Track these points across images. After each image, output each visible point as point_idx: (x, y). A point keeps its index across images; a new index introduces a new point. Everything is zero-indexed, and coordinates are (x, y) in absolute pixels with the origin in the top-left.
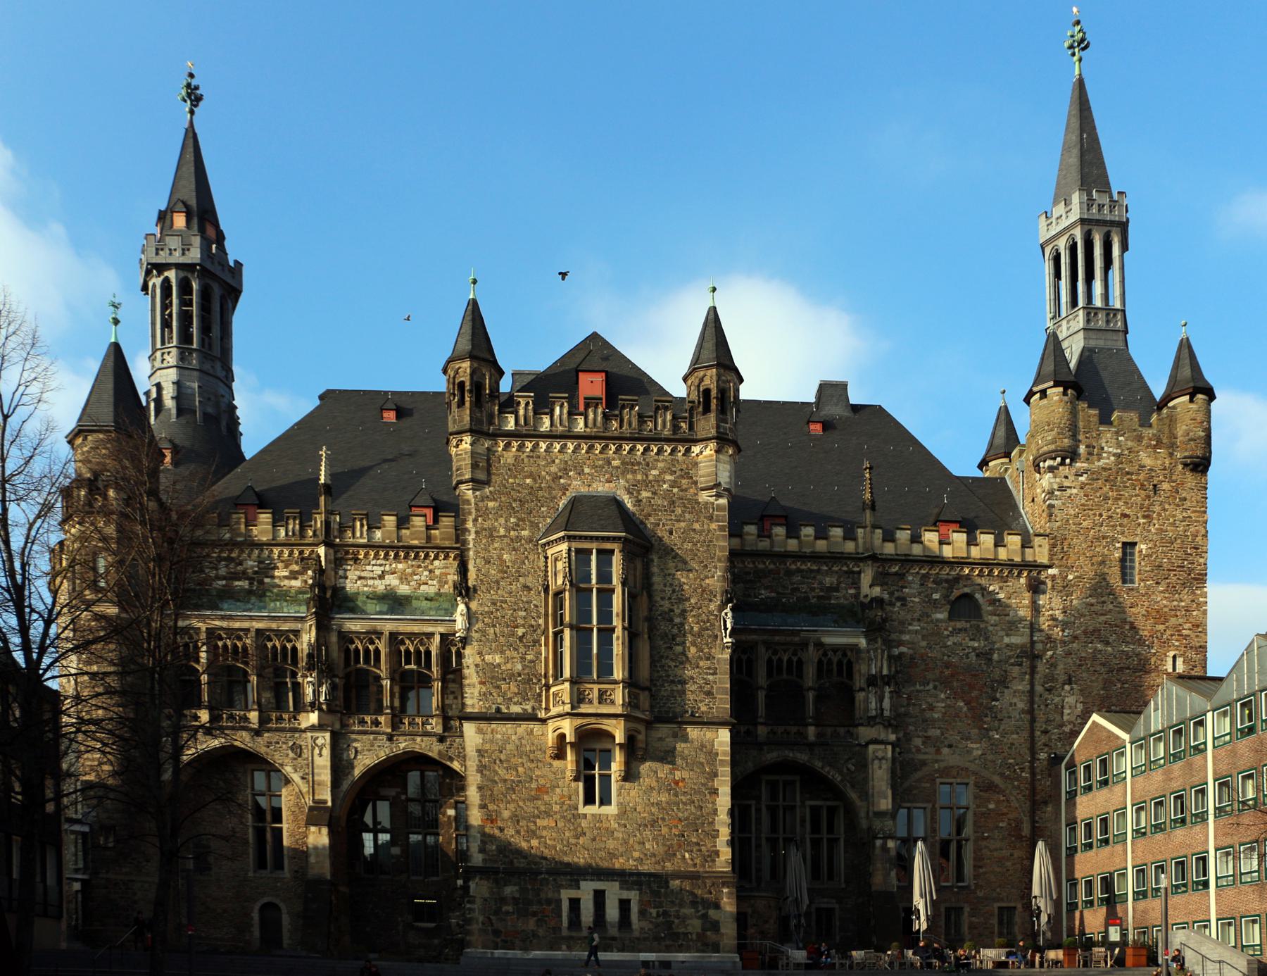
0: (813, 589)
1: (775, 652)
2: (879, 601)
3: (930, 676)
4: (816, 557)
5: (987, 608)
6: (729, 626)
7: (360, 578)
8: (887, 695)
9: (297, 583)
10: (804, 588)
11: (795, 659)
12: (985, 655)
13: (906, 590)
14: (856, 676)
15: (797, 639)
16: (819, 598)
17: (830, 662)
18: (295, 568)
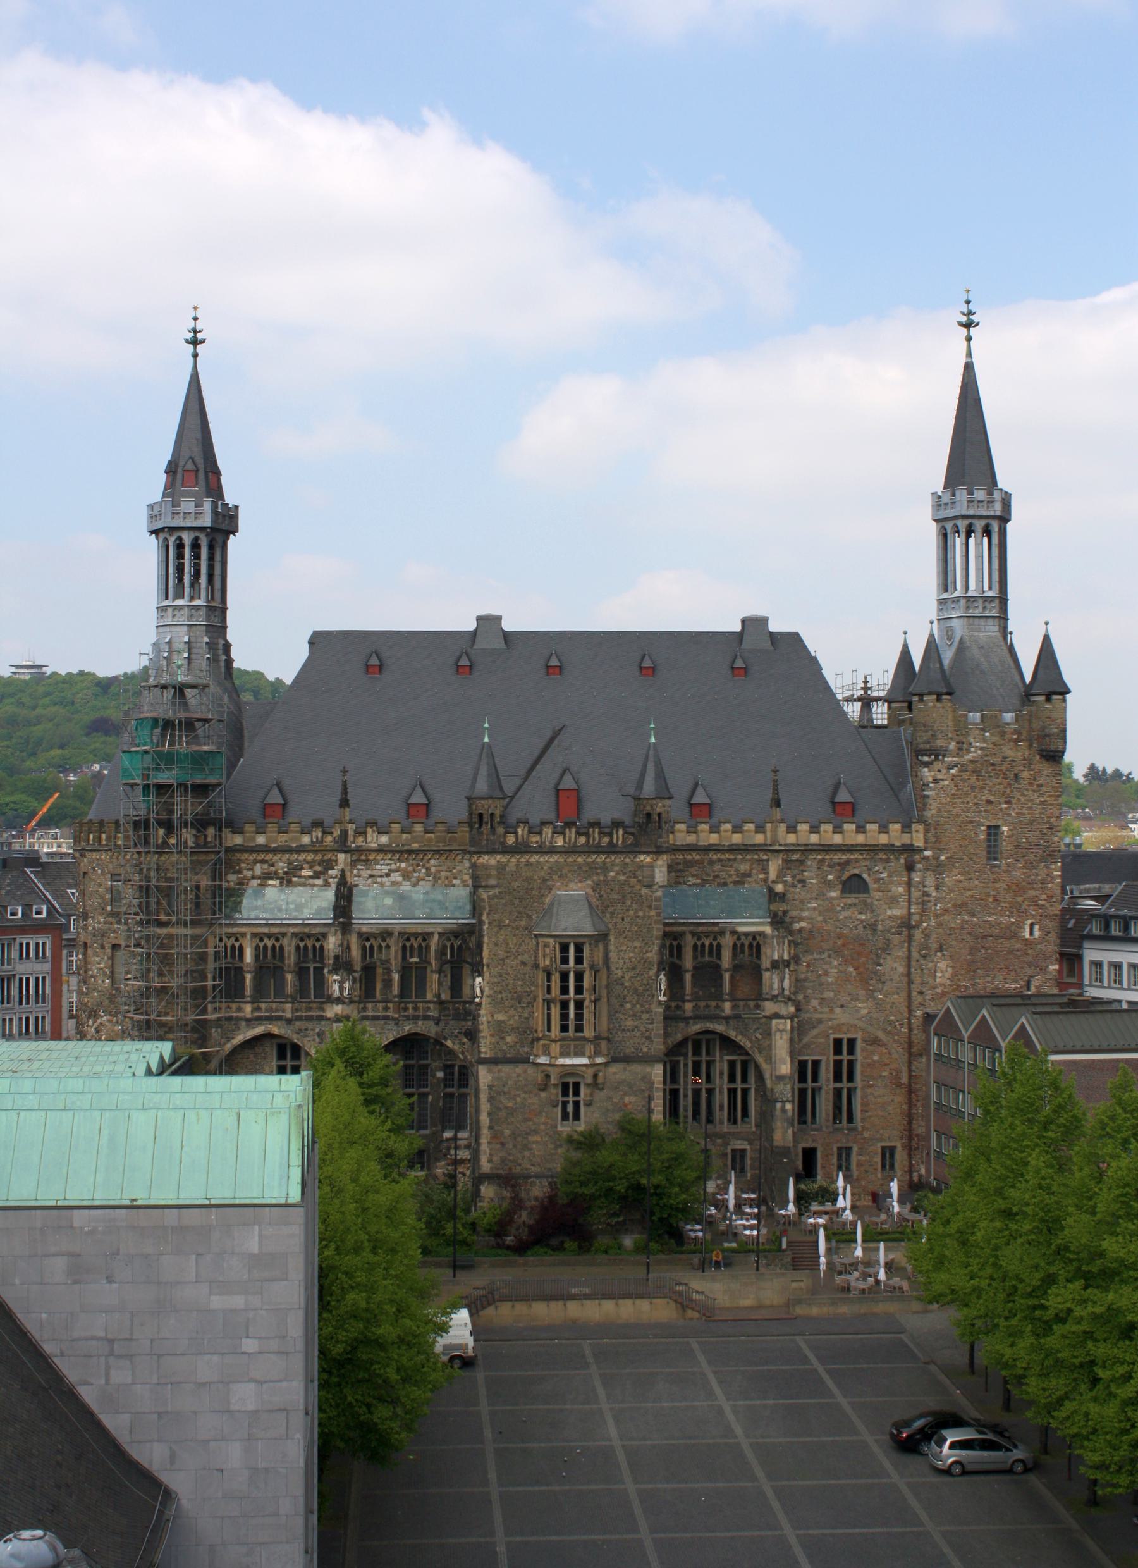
0: (730, 876)
1: (699, 939)
2: (782, 897)
3: (825, 945)
4: (734, 849)
5: (873, 886)
6: (663, 988)
7: (371, 876)
8: (787, 976)
9: (319, 882)
10: (723, 874)
11: (715, 943)
12: (873, 927)
13: (806, 874)
14: (763, 957)
15: (716, 929)
16: (736, 883)
17: (743, 945)
18: (318, 868)
